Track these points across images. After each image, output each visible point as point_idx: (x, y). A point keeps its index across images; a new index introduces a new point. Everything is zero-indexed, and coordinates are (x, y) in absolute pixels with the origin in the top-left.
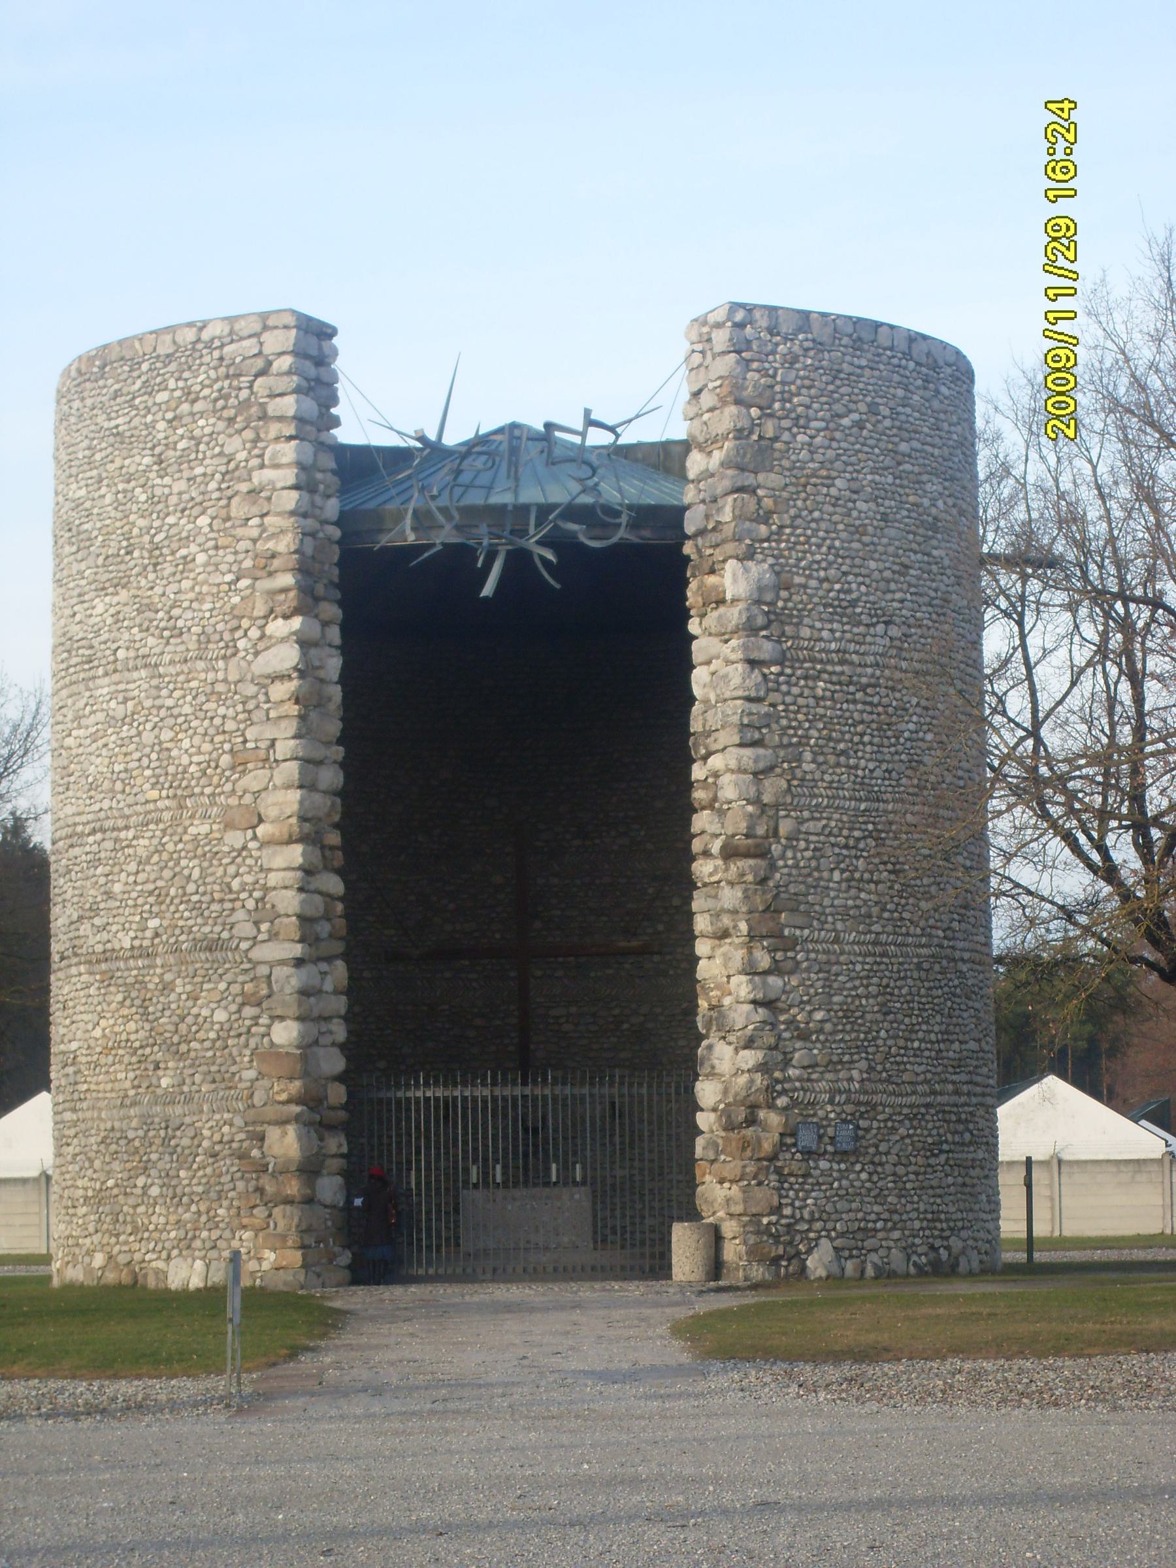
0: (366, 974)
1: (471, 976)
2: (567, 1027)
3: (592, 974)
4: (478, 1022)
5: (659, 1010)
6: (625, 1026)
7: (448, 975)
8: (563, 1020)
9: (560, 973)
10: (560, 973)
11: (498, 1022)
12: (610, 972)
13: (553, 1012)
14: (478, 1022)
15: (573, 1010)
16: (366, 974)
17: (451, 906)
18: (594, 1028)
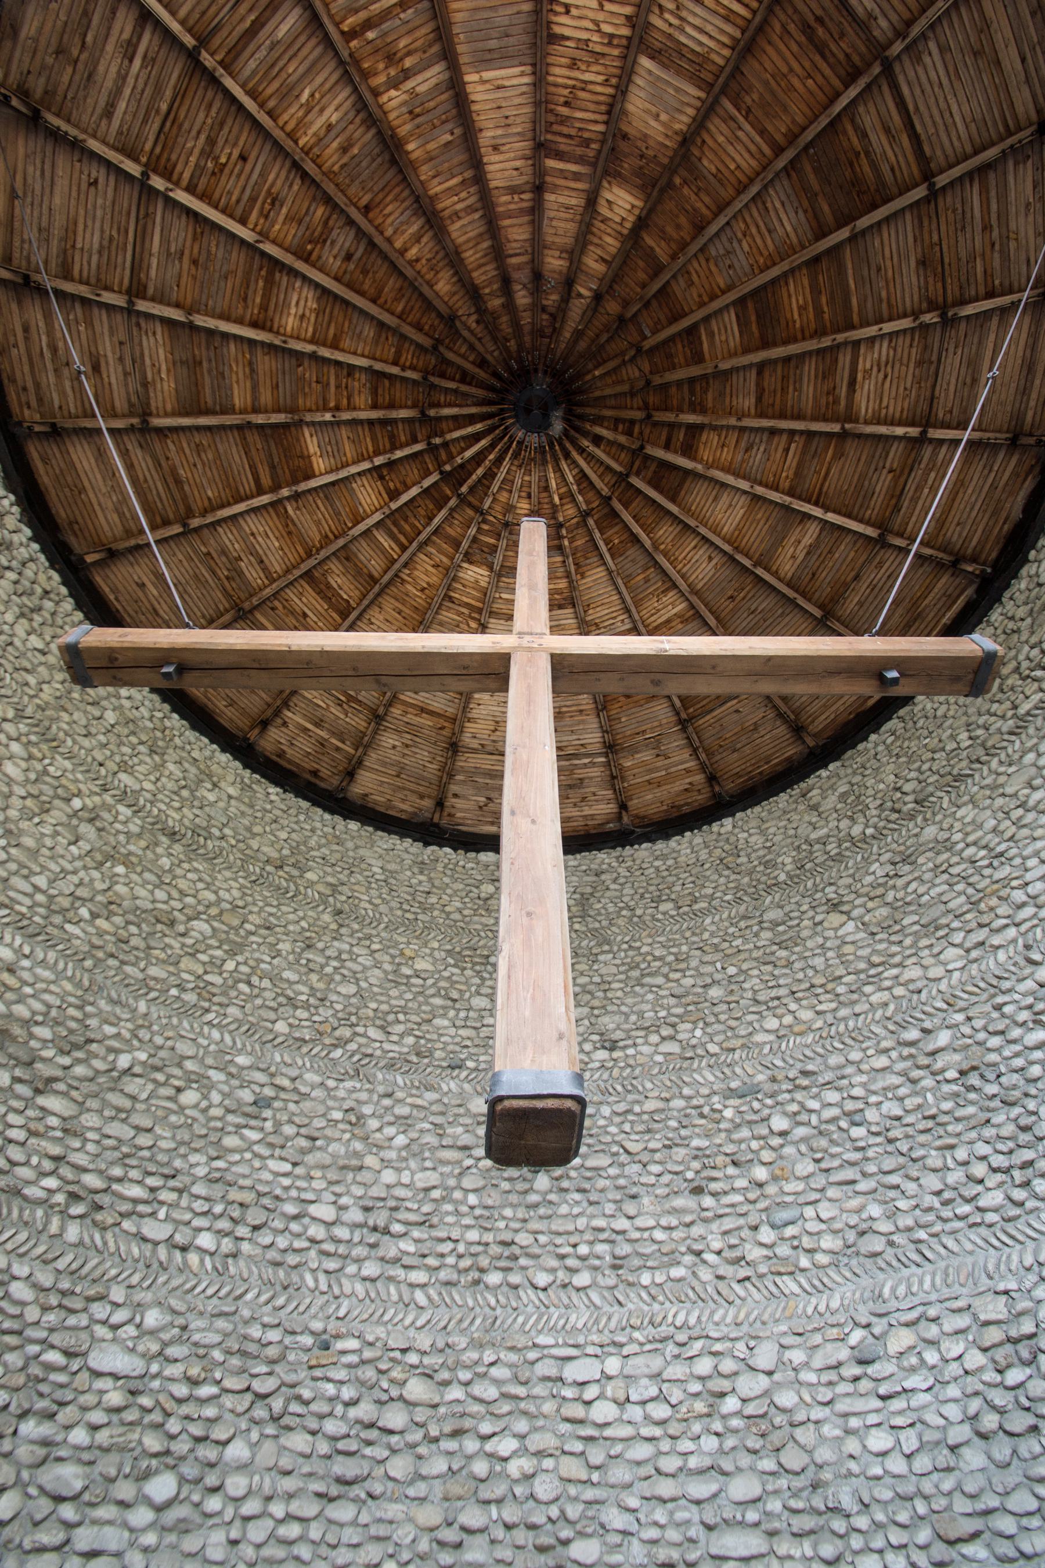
0: (206, 1240)
1: (418, 1276)
2: (603, 1411)
3: (646, 1279)
4: (416, 1389)
5: (797, 1356)
6: (731, 1404)
7: (371, 1269)
8: (591, 1392)
9: (583, 1279)
10: (583, 1279)
11: (456, 1393)
12: (677, 1272)
13: (572, 1372)
14: (416, 1389)
15: (613, 1365)
16: (206, 1240)
17: (401, 1140)
18: (661, 1411)
